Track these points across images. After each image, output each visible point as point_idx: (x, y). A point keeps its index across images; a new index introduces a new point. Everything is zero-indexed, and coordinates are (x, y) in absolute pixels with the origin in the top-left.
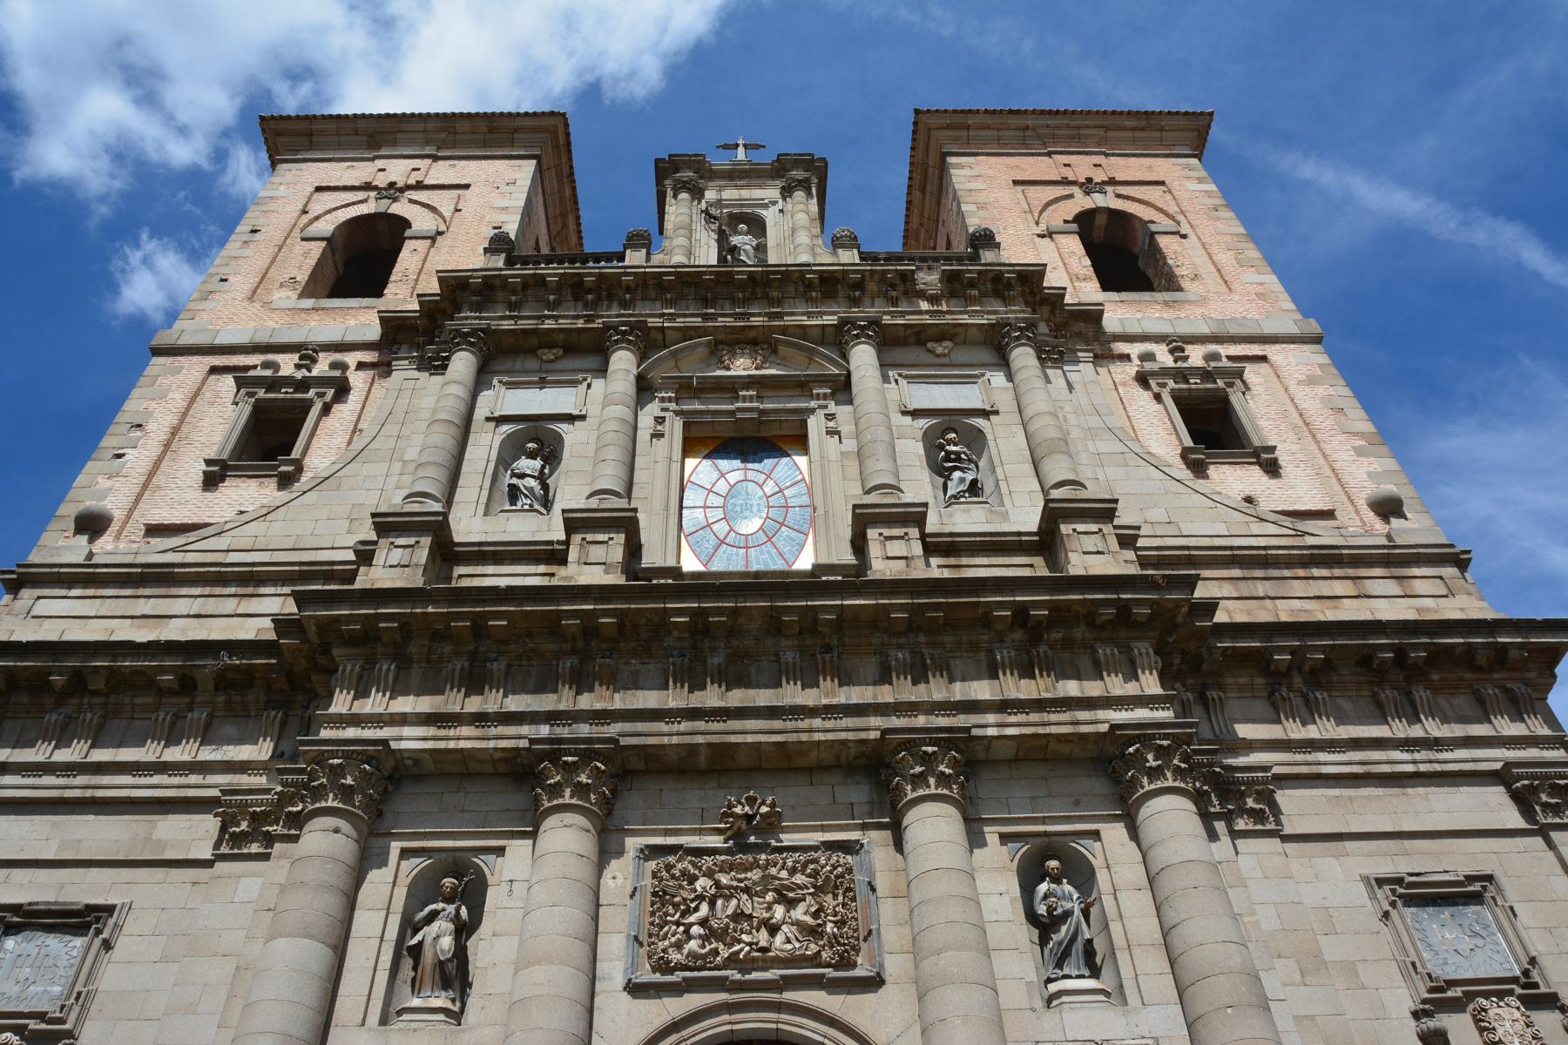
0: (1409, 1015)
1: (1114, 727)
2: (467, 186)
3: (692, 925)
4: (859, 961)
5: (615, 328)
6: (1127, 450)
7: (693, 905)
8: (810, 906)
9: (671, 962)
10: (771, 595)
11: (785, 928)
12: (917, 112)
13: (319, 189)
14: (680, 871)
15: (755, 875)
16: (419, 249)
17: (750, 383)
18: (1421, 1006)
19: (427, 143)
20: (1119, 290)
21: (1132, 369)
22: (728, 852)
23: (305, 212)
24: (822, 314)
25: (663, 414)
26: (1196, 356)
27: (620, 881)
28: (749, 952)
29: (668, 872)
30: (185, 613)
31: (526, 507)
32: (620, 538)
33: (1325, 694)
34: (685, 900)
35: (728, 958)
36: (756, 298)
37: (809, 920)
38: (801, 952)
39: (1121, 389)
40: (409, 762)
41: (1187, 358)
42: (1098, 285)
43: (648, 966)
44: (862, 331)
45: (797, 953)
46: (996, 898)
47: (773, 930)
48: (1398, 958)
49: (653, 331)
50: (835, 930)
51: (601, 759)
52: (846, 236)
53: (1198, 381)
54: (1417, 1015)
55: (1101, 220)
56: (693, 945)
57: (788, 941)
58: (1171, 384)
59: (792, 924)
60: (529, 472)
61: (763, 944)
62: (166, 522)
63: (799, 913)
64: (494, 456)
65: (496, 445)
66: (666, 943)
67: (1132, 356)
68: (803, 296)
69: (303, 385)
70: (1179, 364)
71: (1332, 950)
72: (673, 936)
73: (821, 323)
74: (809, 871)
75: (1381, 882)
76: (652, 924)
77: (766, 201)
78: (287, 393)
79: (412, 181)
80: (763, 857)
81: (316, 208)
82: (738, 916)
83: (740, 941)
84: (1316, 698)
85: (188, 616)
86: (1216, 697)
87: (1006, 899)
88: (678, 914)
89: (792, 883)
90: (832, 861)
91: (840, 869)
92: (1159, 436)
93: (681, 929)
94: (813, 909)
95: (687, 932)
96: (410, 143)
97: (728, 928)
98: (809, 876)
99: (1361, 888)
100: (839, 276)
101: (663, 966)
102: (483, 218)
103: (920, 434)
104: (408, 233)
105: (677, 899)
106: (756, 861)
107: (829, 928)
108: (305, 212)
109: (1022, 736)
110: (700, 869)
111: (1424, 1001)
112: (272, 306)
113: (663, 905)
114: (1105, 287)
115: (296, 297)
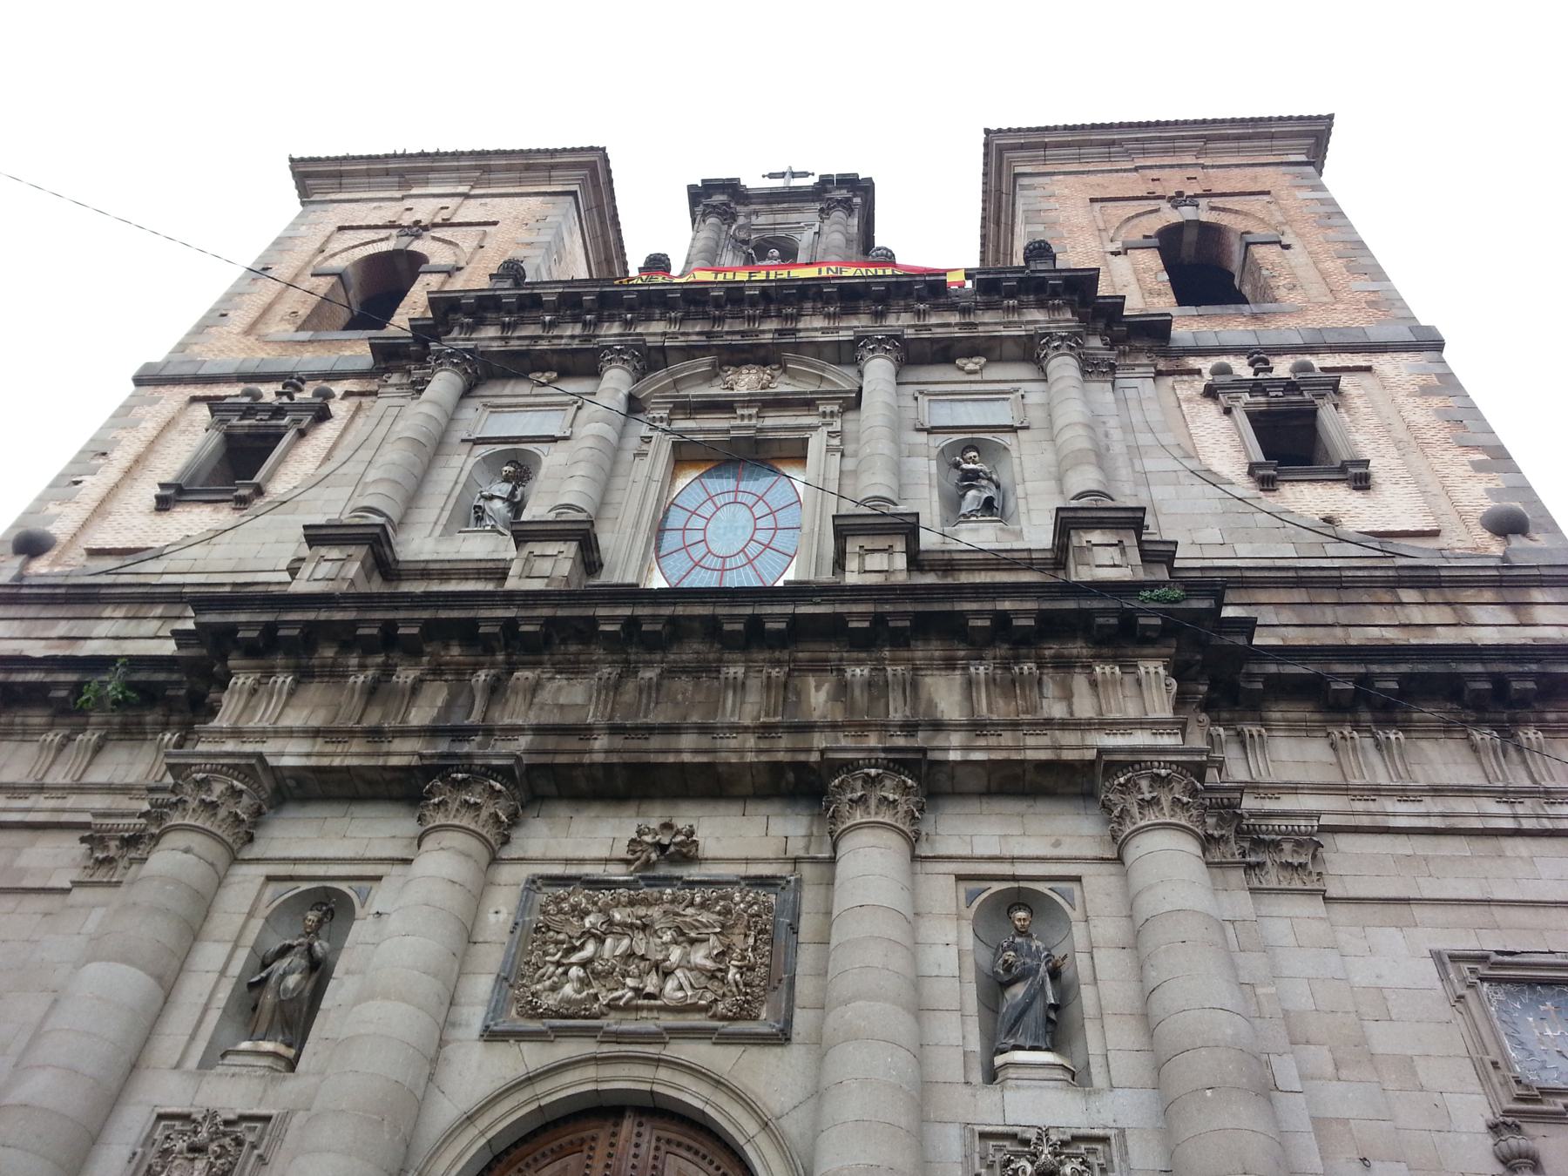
0: (1484, 1129)
1: (1101, 751)
3: (572, 964)
4: (763, 1015)
5: (609, 347)
6: (1181, 468)
7: (578, 944)
8: (714, 948)
9: (540, 1007)
10: (715, 602)
11: (679, 973)
12: (987, 131)
14: (572, 906)
15: (655, 912)
17: (750, 401)
18: (1501, 1119)
20: (1197, 304)
21: (1200, 385)
24: (838, 329)
26: (1282, 367)
27: (502, 916)
28: (631, 999)
29: (557, 904)
30: (104, 635)
31: (489, 528)
32: (570, 548)
33: (1401, 735)
34: (570, 937)
35: (608, 1005)
36: (770, 317)
37: (709, 964)
38: (692, 1001)
39: (1184, 406)
41: (1271, 370)
42: (1175, 300)
43: (513, 1012)
44: (880, 345)
45: (689, 1001)
46: (941, 949)
47: (667, 974)
48: (1475, 1056)
49: (653, 352)
50: (738, 976)
51: (500, 778)
52: (882, 255)
53: (1281, 394)
54: (1494, 1128)
55: (1190, 236)
56: (568, 990)
57: (681, 988)
58: (1246, 397)
59: (691, 970)
60: (498, 494)
61: (650, 989)
62: (107, 547)
63: (699, 956)
66: (539, 987)
67: (1203, 371)
68: (821, 313)
70: (1261, 376)
71: (1383, 1039)
72: (549, 978)
73: (837, 339)
74: (718, 908)
75: (1454, 958)
76: (527, 963)
77: (802, 224)
78: (261, 420)
80: (669, 891)
82: (630, 955)
84: (1388, 738)
85: (106, 638)
86: (1255, 734)
87: (953, 951)
88: (560, 954)
89: (698, 921)
90: (748, 899)
91: (756, 907)
92: (1225, 454)
93: (560, 970)
94: (715, 952)
95: (565, 973)
97: (614, 969)
98: (719, 913)
99: (1430, 967)
103: (935, 452)
105: (561, 937)
107: (732, 974)
109: (990, 761)
110: (595, 903)
111: (1507, 1113)
113: (544, 943)
114: (1181, 301)
115: (294, 329)
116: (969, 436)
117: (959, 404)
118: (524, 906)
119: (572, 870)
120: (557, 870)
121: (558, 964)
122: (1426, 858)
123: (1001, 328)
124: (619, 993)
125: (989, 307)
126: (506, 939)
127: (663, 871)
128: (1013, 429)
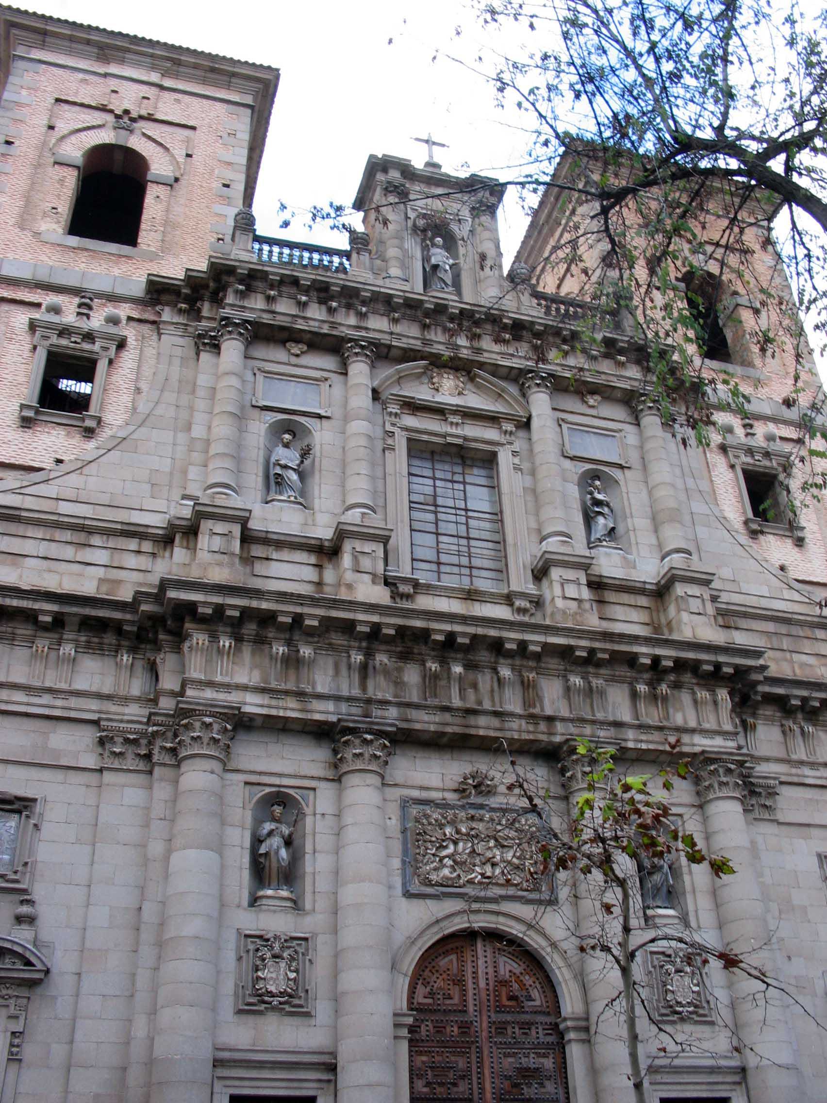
2: (193, 128)
15: (481, 826)
16: (162, 197)
19: (153, 68)
22: (463, 807)
25: (392, 429)
35: (467, 881)
40: (245, 719)
47: (494, 865)
56: (446, 872)
61: (489, 874)
79: (144, 113)
83: (473, 871)
93: (438, 859)
95: (441, 860)
96: (137, 65)
100: (527, 325)
101: (429, 883)
102: (213, 170)
105: (434, 839)
106: (483, 816)
116: (594, 467)
117: (585, 434)
118: (404, 817)
119: (425, 795)
120: (416, 794)
122: (817, 801)
123: (615, 379)
124: (473, 875)
125: (606, 356)
127: (479, 800)
128: (621, 467)
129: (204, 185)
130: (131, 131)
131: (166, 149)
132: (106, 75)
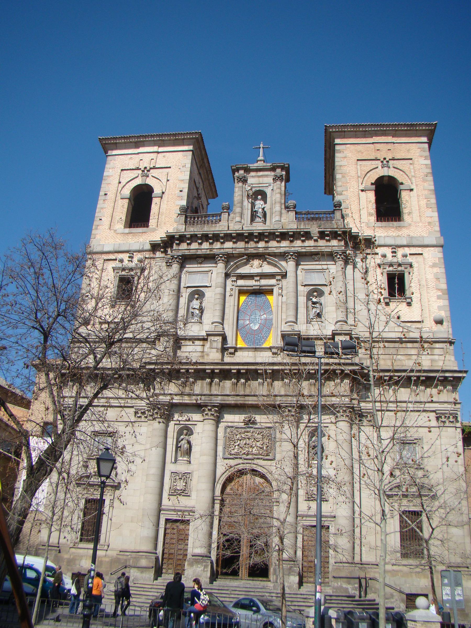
2: (170, 167)
13: (122, 170)
23: (120, 183)
27: (221, 434)
56: (236, 450)
64: (187, 300)
65: (187, 297)
69: (131, 269)
79: (152, 166)
81: (124, 182)
104: (153, 195)
108: (120, 183)
112: (118, 232)
118: (225, 432)
120: (230, 424)
121: (233, 445)
126: (223, 439)
129: (173, 193)
130: (148, 176)
131: (160, 180)
132: (138, 153)
